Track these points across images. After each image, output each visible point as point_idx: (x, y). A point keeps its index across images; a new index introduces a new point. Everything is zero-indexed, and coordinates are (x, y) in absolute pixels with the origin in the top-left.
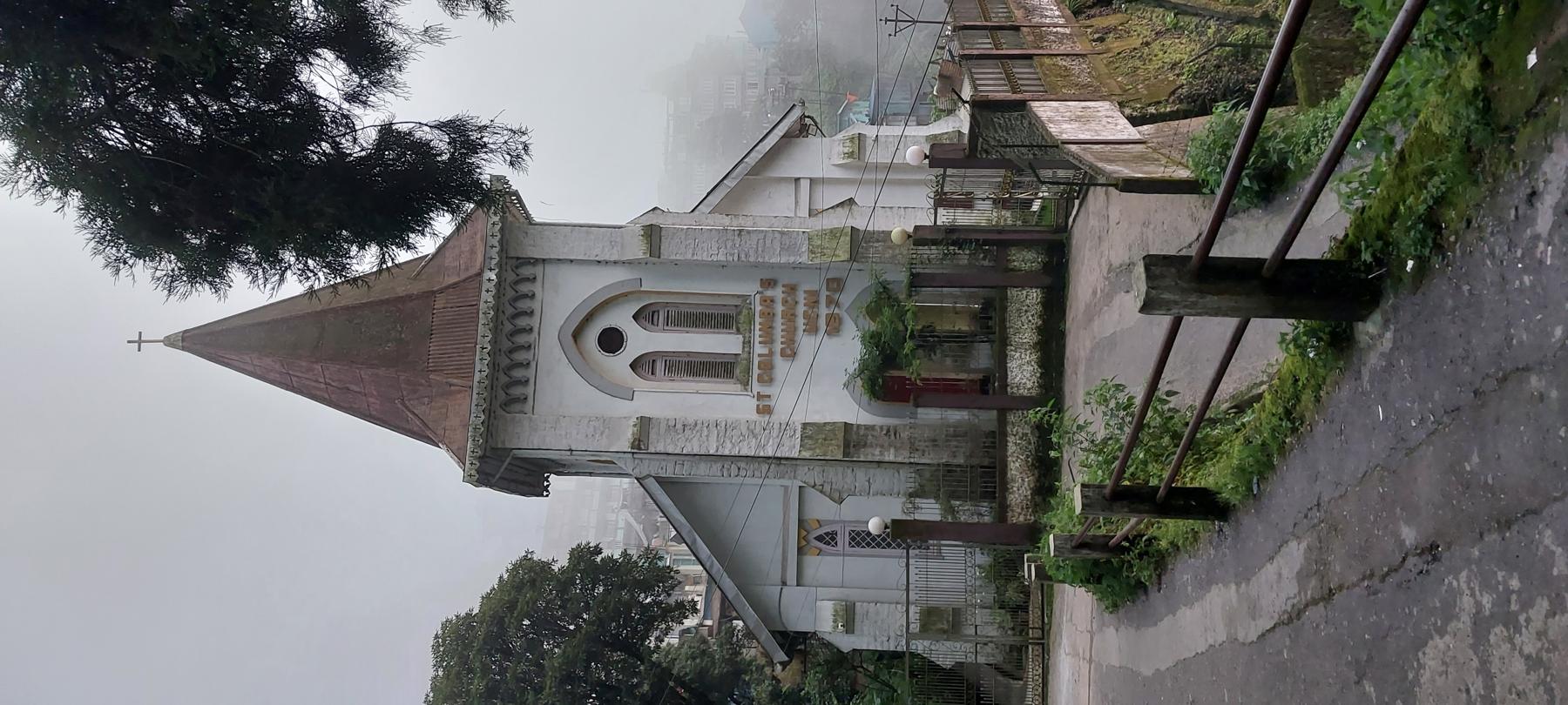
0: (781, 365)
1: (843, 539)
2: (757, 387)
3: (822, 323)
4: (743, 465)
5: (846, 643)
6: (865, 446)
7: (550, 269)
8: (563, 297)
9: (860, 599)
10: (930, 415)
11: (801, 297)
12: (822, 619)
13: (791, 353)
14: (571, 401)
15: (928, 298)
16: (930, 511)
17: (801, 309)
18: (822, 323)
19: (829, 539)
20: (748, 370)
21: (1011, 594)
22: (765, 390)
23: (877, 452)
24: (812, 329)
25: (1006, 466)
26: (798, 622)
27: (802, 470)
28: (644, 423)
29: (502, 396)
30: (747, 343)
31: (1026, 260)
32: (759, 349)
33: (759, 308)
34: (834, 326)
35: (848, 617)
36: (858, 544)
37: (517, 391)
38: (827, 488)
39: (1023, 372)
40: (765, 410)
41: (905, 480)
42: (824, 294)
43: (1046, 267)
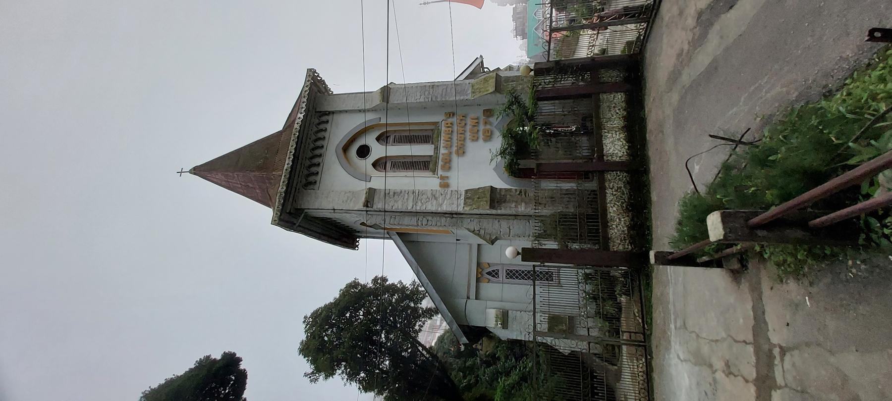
0: (455, 157)
1: (502, 274)
2: (440, 172)
3: (481, 133)
4: (430, 218)
5: (504, 335)
6: (505, 202)
7: (335, 116)
8: (341, 130)
9: (512, 308)
10: (549, 185)
11: (469, 122)
12: (490, 320)
13: (461, 151)
14: (340, 187)
15: (547, 107)
16: (551, 245)
17: (468, 127)
18: (481, 133)
19: (494, 274)
20: (436, 163)
21: (609, 308)
22: (445, 174)
23: (513, 205)
24: (475, 139)
25: (605, 211)
26: (476, 321)
27: (466, 222)
28: (371, 192)
29: (304, 181)
30: (437, 149)
31: (611, 76)
32: (443, 151)
33: (443, 129)
34: (489, 137)
35: (504, 319)
36: (511, 277)
37: (311, 179)
38: (482, 232)
39: (615, 146)
40: (445, 185)
41: (532, 227)
42: (482, 118)
43: (626, 80)
